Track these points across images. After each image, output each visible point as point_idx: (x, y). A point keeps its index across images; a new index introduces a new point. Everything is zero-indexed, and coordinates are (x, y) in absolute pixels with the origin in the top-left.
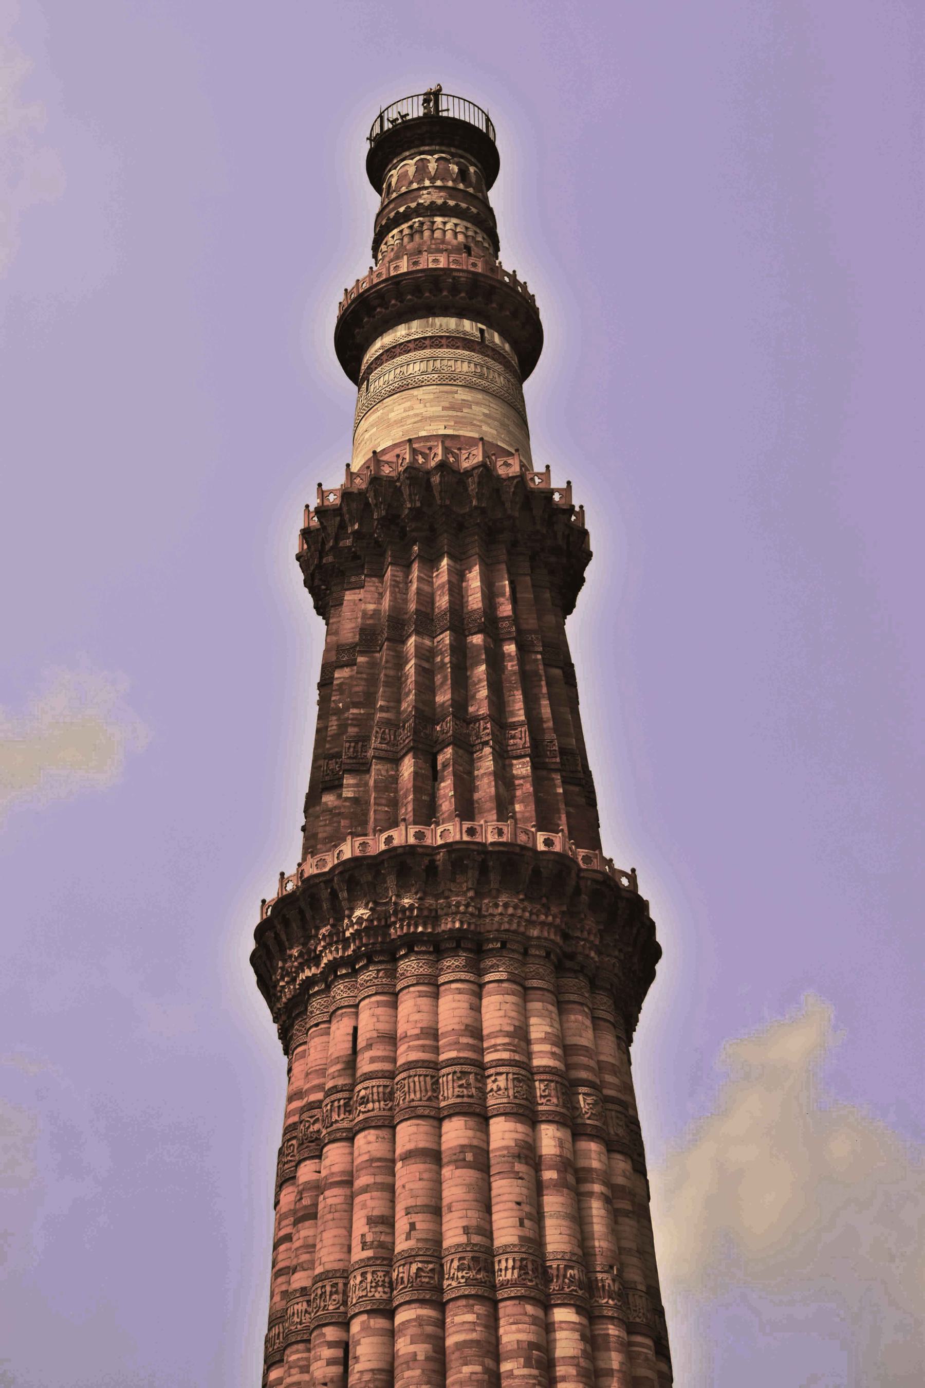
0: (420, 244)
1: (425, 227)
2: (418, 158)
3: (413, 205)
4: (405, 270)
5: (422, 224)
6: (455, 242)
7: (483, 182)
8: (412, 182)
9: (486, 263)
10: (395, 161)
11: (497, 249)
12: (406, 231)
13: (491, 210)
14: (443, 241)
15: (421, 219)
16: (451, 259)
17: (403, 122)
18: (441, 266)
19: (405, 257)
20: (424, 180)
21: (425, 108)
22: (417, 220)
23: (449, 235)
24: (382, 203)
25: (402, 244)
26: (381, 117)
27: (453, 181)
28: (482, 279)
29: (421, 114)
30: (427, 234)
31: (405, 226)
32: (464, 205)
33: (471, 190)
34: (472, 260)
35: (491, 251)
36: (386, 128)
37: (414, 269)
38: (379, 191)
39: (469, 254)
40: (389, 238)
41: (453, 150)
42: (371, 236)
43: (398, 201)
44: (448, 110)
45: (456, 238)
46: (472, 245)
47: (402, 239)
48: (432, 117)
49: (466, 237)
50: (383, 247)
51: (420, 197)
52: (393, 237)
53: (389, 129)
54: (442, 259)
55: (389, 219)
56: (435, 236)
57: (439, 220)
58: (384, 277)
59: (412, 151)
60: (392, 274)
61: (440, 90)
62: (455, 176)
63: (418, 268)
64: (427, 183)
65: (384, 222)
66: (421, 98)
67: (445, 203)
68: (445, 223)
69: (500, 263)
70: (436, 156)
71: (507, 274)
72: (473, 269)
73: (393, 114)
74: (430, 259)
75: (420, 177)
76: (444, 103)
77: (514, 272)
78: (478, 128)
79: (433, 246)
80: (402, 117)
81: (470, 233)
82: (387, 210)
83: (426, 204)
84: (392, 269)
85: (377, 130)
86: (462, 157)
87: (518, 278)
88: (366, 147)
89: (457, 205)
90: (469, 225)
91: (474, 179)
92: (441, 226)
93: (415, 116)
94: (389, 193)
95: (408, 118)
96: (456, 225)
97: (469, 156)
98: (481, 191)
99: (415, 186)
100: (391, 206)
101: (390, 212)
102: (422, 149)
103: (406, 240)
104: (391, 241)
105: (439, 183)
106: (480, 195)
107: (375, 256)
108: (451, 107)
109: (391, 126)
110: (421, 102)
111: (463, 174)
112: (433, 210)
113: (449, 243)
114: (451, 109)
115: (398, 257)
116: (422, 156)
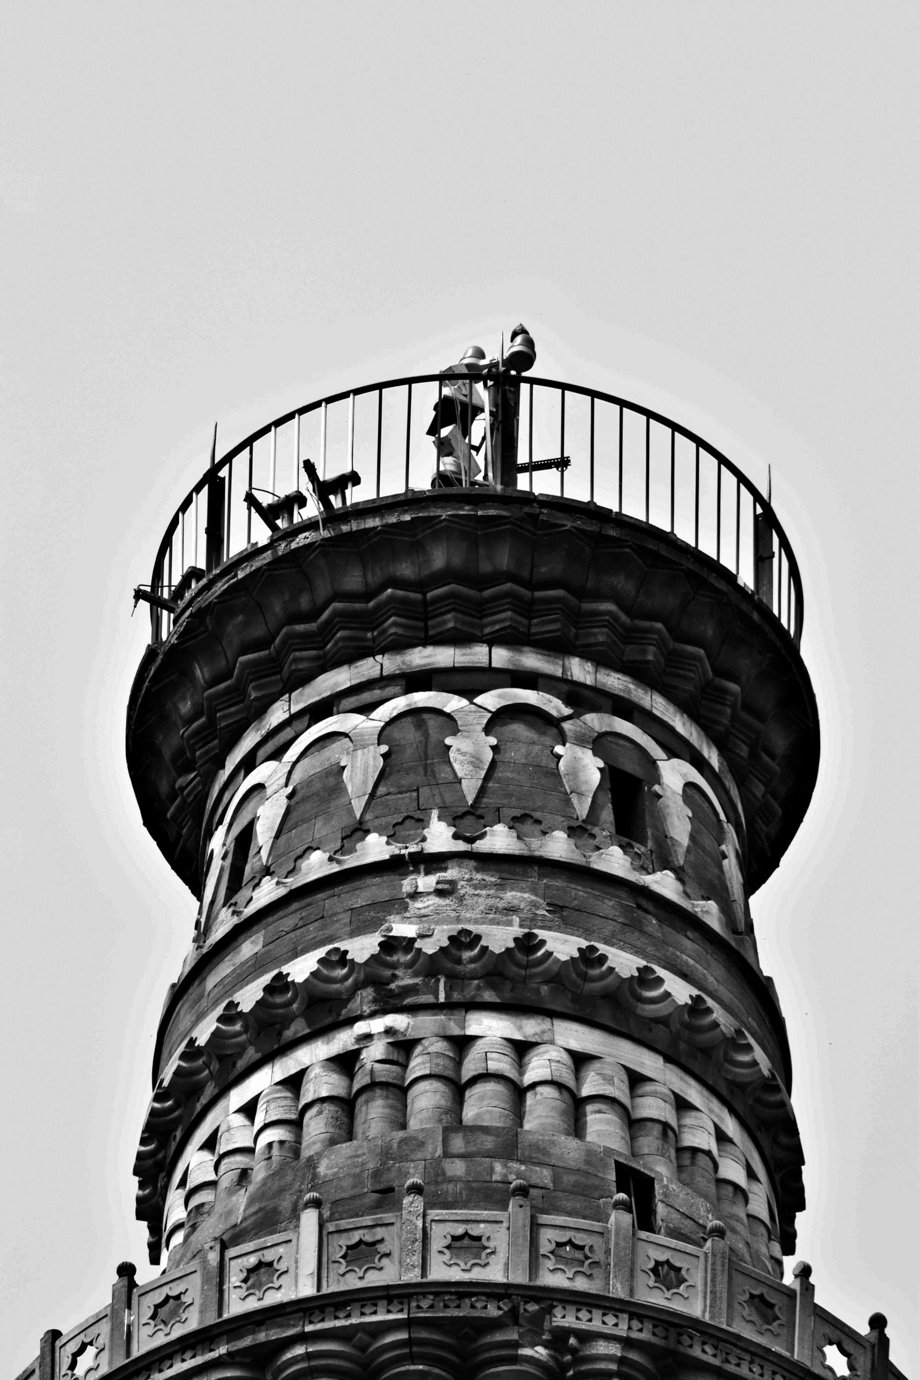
0: (386, 1154)
1: (418, 1065)
2: (399, 704)
3: (363, 948)
4: (307, 1289)
5: (403, 1047)
6: (569, 1150)
7: (731, 846)
8: (359, 830)
9: (732, 1265)
10: (277, 714)
11: (790, 1197)
12: (323, 1084)
13: (761, 994)
14: (510, 1144)
15: (399, 1021)
16: (548, 1238)
17: (331, 517)
18: (494, 1273)
19: (309, 1219)
20: (422, 822)
21: (444, 448)
22: (377, 1025)
23: (542, 1111)
24: (202, 930)
25: (294, 1149)
26: (214, 483)
27: (576, 831)
28: (705, 1354)
29: (422, 482)
30: (426, 1100)
31: (312, 1055)
32: (624, 962)
33: (664, 884)
34: (656, 1248)
35: (760, 1202)
36: (236, 545)
37: (353, 1282)
38: (189, 866)
39: (645, 1219)
40: (226, 1118)
41: (580, 671)
42: (139, 1102)
43: (286, 921)
44: (562, 463)
45: (577, 1128)
46: (661, 1170)
47: (296, 1125)
48: (479, 497)
49: (634, 1125)
50: (196, 1162)
51: (398, 905)
52: (249, 1110)
53: (255, 552)
54: (499, 1239)
55: (230, 1015)
56: (470, 1113)
57: (490, 1028)
58: (192, 1322)
59: (368, 668)
60: (238, 1304)
61: (524, 358)
62: (582, 808)
63: (374, 1279)
64: (439, 837)
65: (203, 1034)
66: (427, 397)
67: (527, 944)
68: (521, 1049)
69: (805, 1272)
70: (491, 700)
71: (836, 1331)
72: (658, 1299)
73: (275, 472)
74: (440, 1236)
75: (406, 802)
76: (541, 423)
77: (878, 1322)
78: (714, 566)
79: (457, 1168)
80: (324, 489)
81: (652, 1107)
82: (224, 969)
83: (429, 947)
84: (234, 1278)
85: (190, 551)
86: (624, 708)
87: (893, 1357)
88: (133, 635)
89: (589, 957)
90: (649, 1063)
91: (679, 826)
92: (501, 1064)
93: (393, 487)
94: (236, 881)
95: (357, 495)
96: (580, 1060)
97: (659, 706)
98: (715, 890)
99: (375, 848)
100: (249, 948)
101: (242, 978)
102: (422, 657)
103: (316, 1126)
104: (237, 1133)
105: (499, 839)
106: (710, 912)
107: (150, 1210)
108: (577, 452)
109: (262, 534)
110: (425, 415)
111: (628, 798)
112: (468, 976)
113: (538, 1155)
114: (578, 459)
115: (269, 1219)
116: (421, 699)
